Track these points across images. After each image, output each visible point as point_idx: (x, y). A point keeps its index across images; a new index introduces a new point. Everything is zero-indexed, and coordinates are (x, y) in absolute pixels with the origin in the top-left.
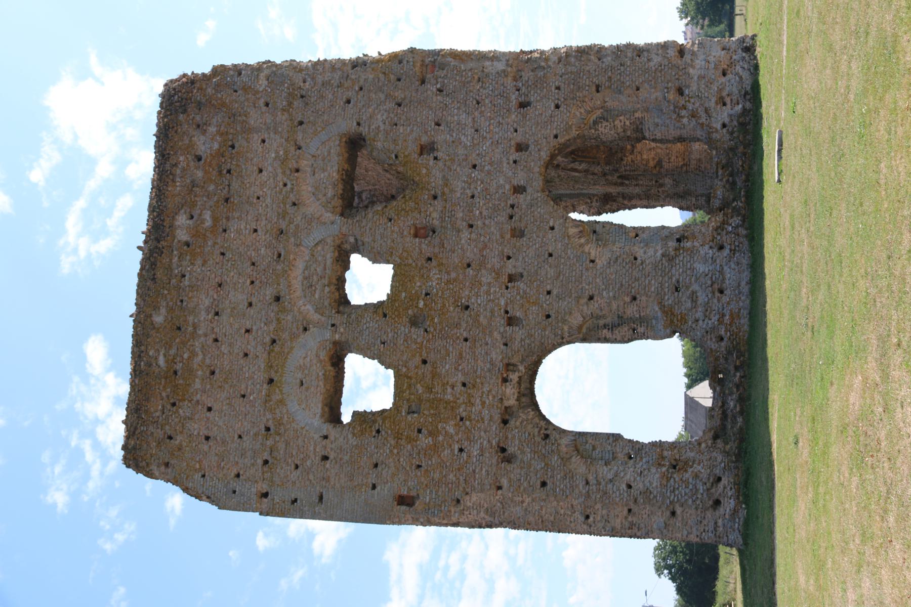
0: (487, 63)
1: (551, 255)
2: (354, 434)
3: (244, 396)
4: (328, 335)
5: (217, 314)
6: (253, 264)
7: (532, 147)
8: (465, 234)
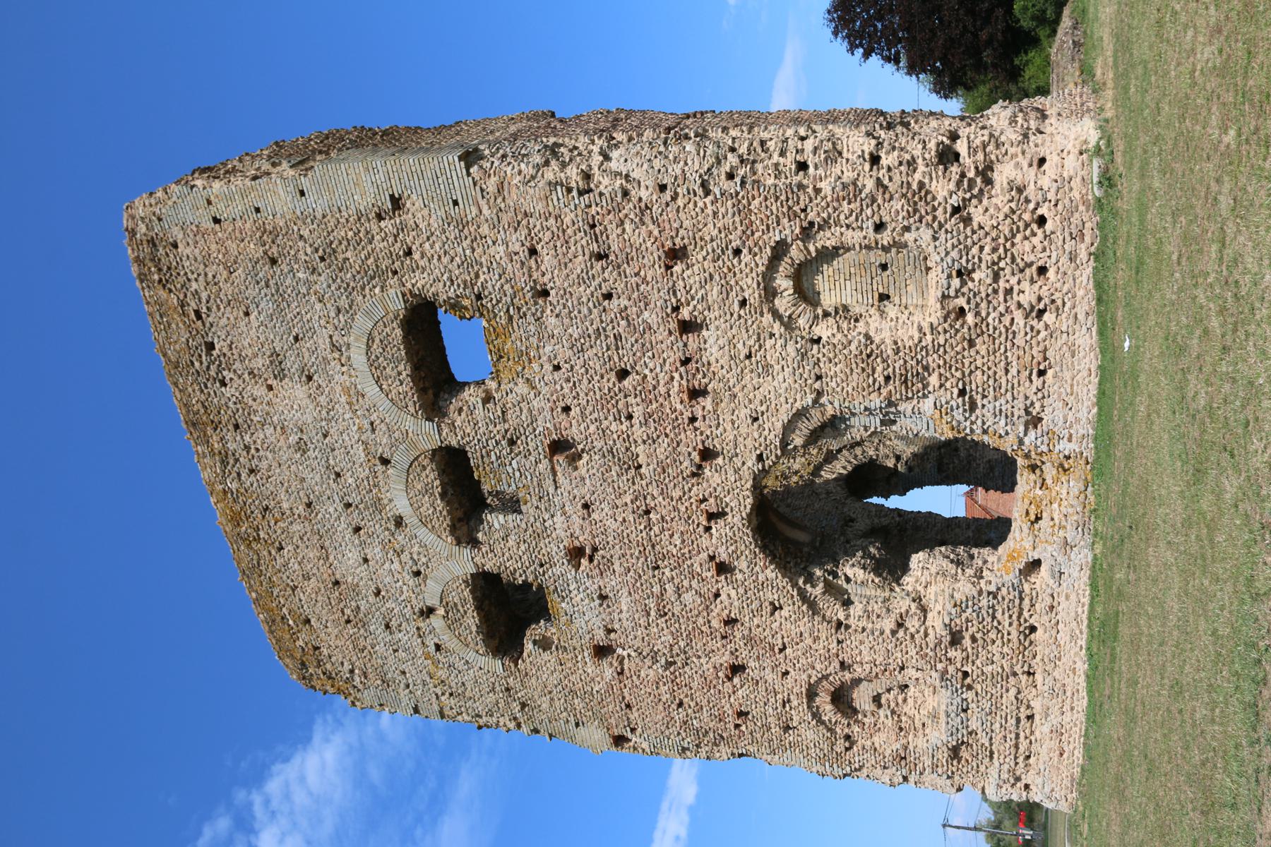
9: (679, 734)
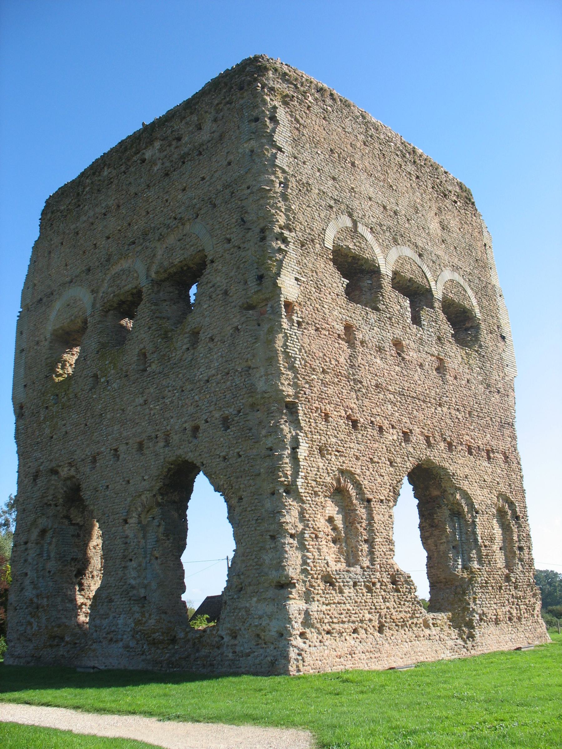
0: (262, 370)
1: (128, 482)
2: (47, 359)
3: (66, 265)
4: (89, 312)
5: (105, 215)
6: (130, 224)
7: (195, 441)
8: (140, 400)
9: (303, 359)
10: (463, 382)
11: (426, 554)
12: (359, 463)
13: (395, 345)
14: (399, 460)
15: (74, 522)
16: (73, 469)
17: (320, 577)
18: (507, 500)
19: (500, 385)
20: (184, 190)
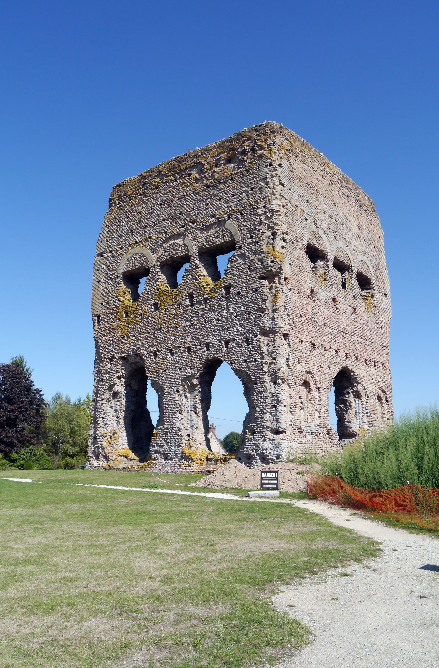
1: (180, 369)
5: (161, 204)
10: (365, 322)
11: (337, 419)
12: (315, 368)
13: (333, 300)
14: (333, 366)
15: (132, 388)
16: (138, 358)
17: (297, 429)
18: (384, 392)
19: (383, 324)
20: (220, 200)
